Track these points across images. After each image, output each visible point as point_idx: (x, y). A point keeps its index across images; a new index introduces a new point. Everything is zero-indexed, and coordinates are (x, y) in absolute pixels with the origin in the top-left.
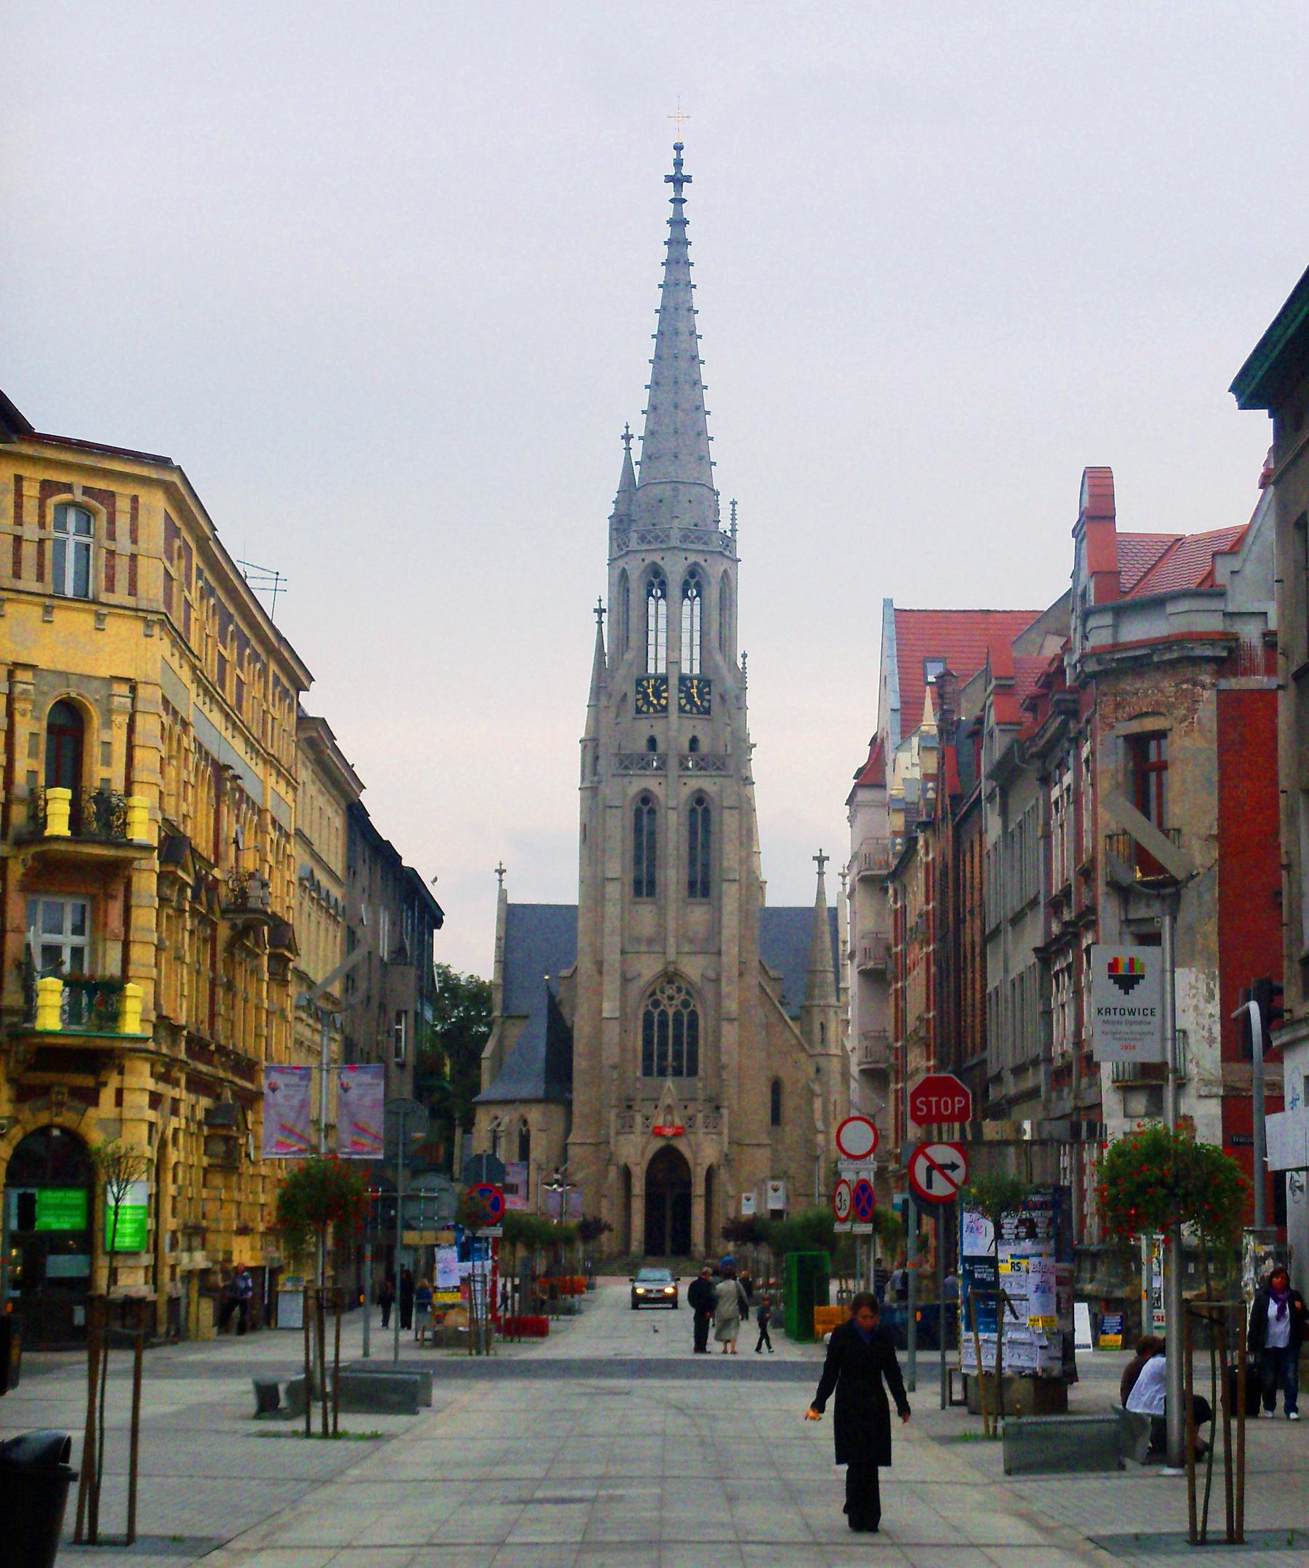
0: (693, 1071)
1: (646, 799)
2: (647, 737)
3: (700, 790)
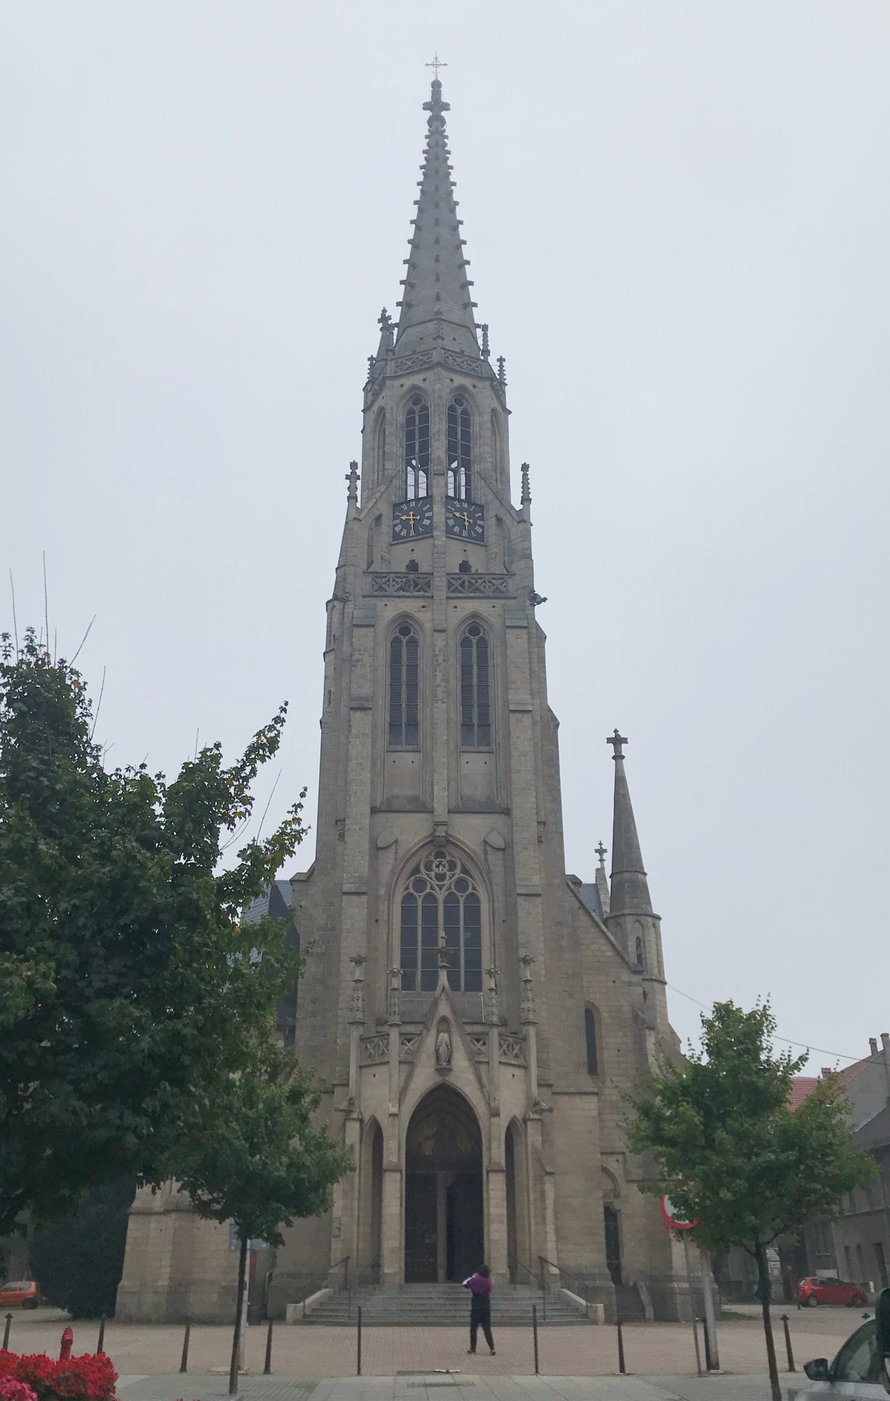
1: (405, 627)
2: (407, 563)
3: (475, 615)
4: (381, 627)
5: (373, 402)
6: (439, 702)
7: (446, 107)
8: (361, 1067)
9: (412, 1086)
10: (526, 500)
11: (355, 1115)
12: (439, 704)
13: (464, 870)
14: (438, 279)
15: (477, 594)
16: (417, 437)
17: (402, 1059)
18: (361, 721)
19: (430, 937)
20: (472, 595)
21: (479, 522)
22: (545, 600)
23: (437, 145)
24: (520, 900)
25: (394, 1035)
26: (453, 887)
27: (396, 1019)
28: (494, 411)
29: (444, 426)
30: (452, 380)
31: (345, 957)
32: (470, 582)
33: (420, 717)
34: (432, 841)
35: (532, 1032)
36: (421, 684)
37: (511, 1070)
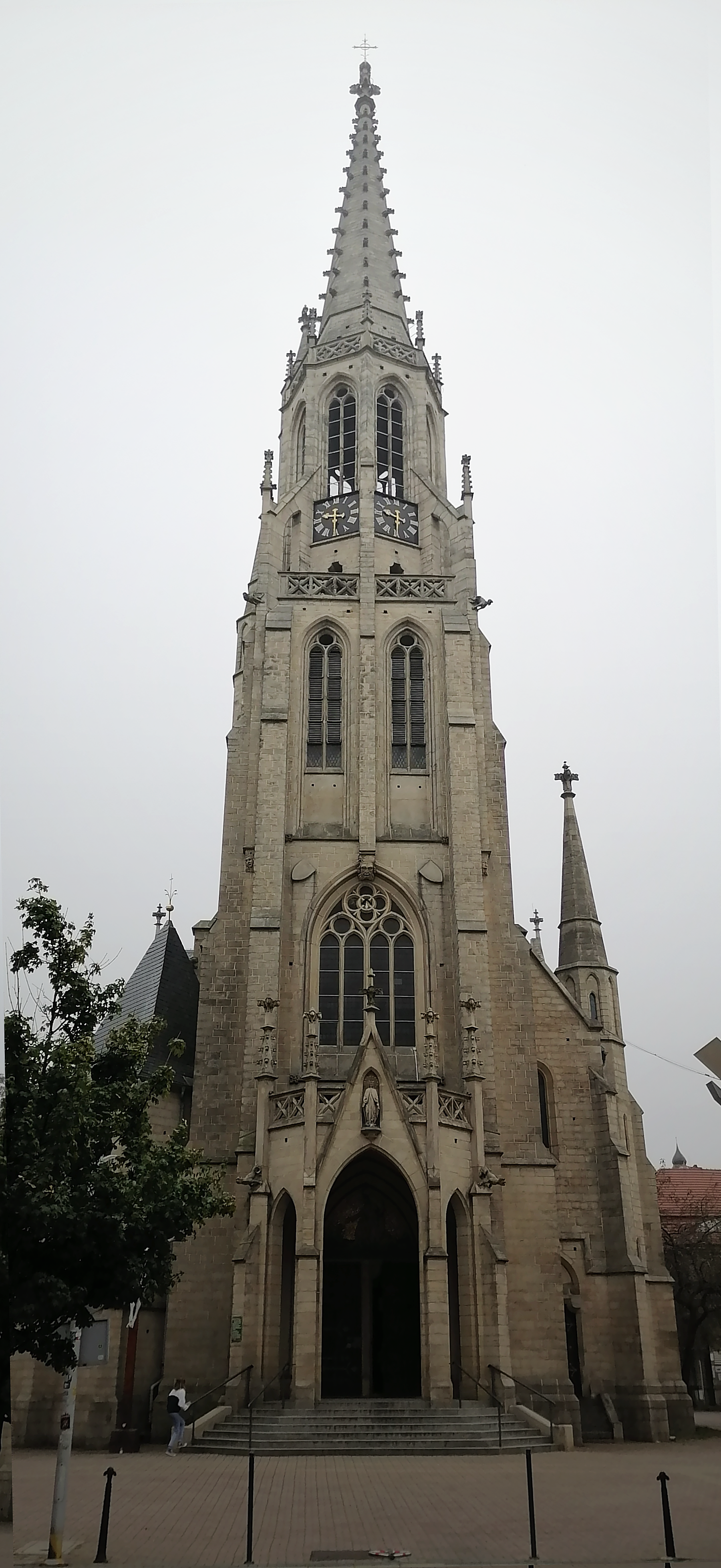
0: (407, 1037)
1: (326, 635)
3: (408, 622)
4: (299, 633)
5: (291, 399)
6: (367, 717)
7: (376, 90)
8: (270, 1131)
9: (332, 1152)
10: (467, 494)
11: (261, 1189)
12: (366, 719)
13: (395, 907)
14: (366, 264)
15: (411, 598)
16: (342, 429)
17: (320, 1118)
18: (273, 735)
19: (355, 982)
20: (405, 598)
21: (412, 522)
22: (490, 602)
23: (365, 127)
24: (462, 938)
25: (311, 1089)
26: (381, 926)
27: (313, 1072)
28: (428, 407)
29: (373, 416)
30: (382, 368)
31: (252, 1003)
32: (401, 584)
33: (343, 735)
34: (356, 874)
35: (477, 1088)
36: (344, 699)
37: (453, 1134)
